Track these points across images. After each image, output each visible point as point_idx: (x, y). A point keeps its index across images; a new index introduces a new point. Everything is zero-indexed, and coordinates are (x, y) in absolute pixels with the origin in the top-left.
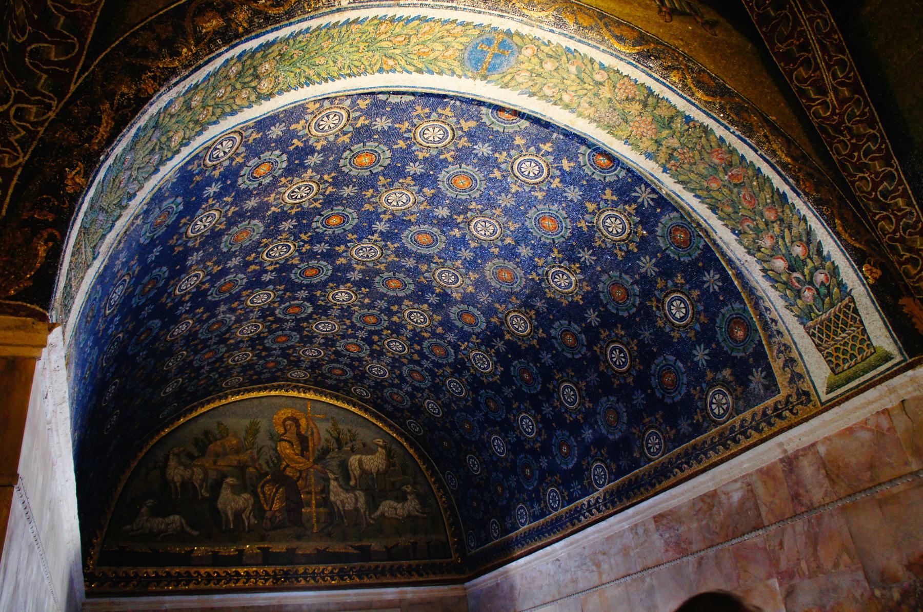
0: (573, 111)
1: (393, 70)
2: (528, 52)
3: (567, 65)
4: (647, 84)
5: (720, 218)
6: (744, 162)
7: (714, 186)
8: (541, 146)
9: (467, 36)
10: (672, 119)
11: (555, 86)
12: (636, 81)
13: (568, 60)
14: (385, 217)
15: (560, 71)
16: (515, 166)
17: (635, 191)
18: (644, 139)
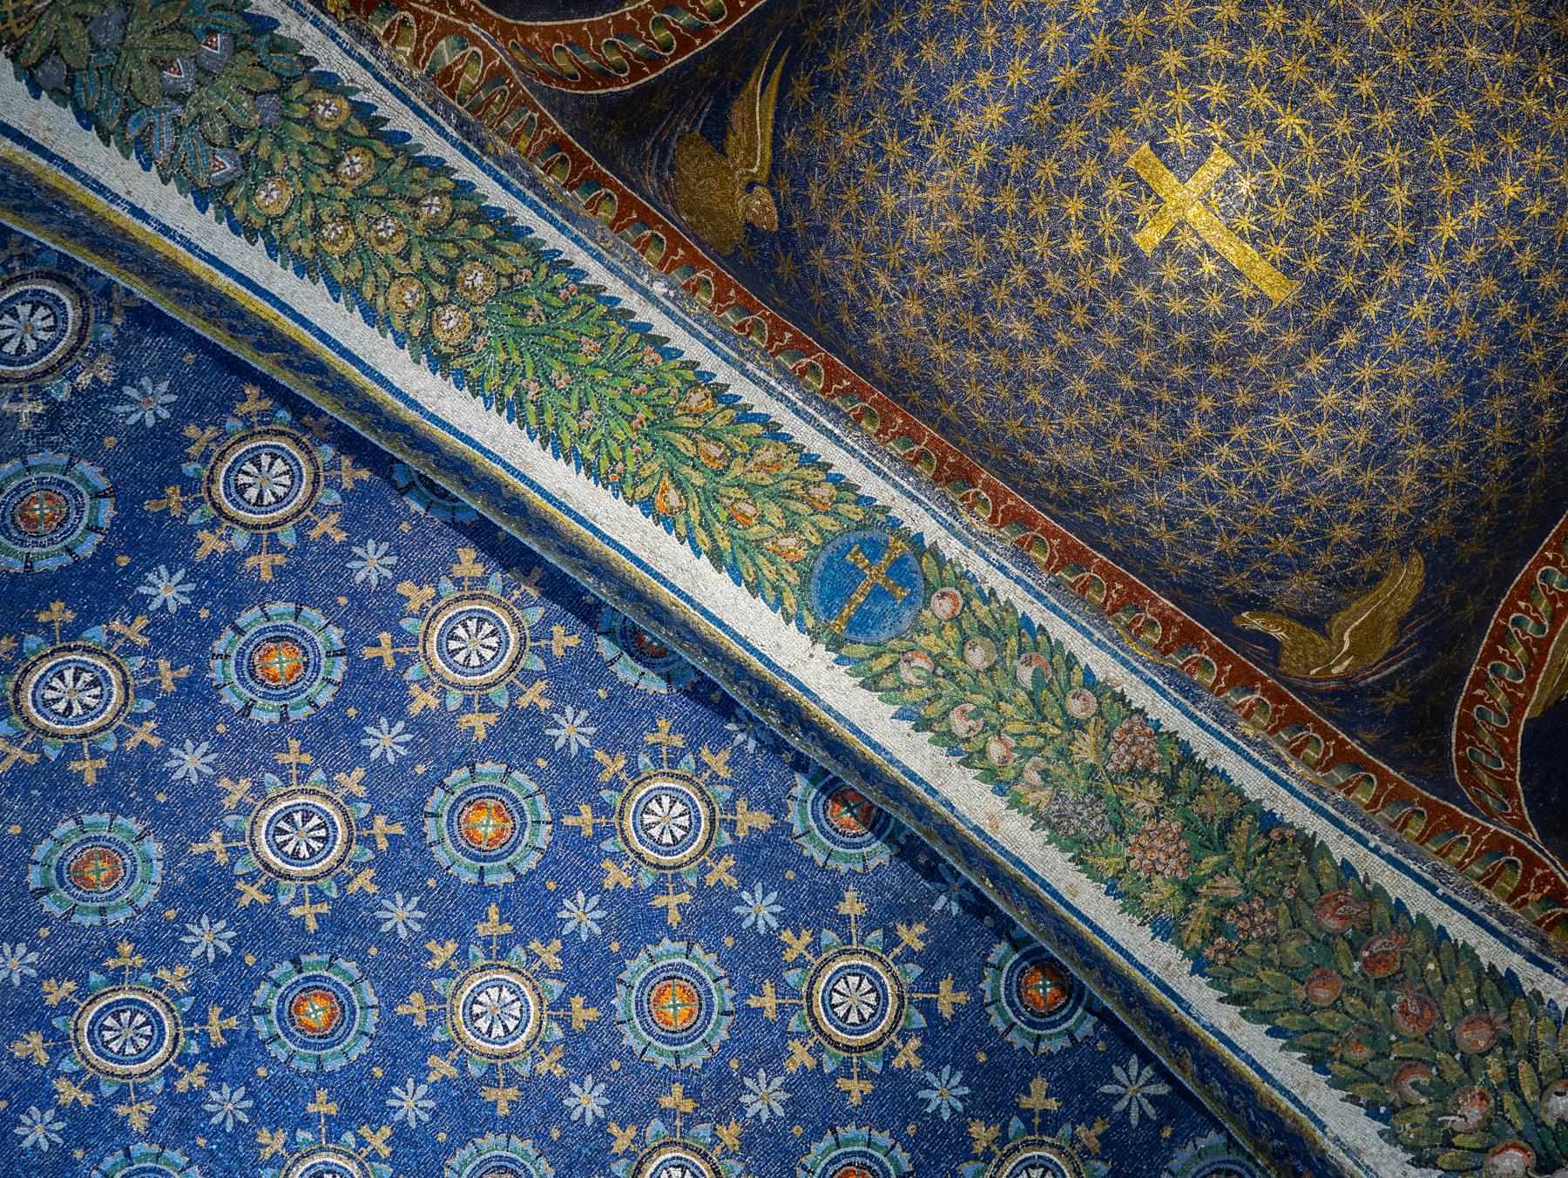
0: (1000, 791)
1: (666, 521)
2: (943, 607)
3: (1016, 663)
4: (1182, 736)
5: (1336, 1084)
6: (1402, 919)
8: (902, 930)
9: (836, 514)
10: (1228, 826)
11: (978, 713)
12: (1158, 725)
13: (1021, 652)
14: (442, 1067)
15: (998, 674)
16: (821, 985)
17: (1112, 1079)
18: (1158, 880)
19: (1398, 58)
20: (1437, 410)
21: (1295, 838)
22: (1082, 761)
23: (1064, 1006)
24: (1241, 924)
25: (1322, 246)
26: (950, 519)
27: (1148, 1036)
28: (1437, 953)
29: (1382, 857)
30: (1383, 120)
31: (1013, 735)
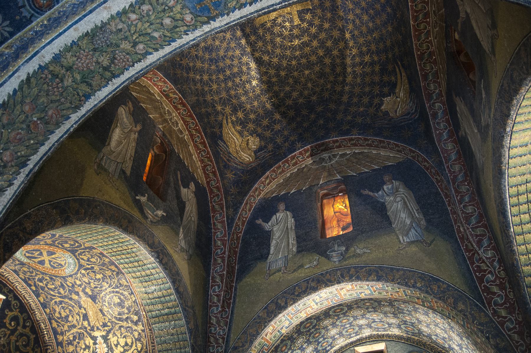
0: (118, 13)
2: (188, 17)
3: (161, 33)
4: (121, 76)
7: (27, 108)
11: (148, 15)
12: (127, 69)
13: (165, 36)
18: (75, 59)
19: (296, 73)
20: (211, 50)
21: (81, 104)
22: (122, 44)
23: (35, 6)
24: (54, 84)
25: (263, 35)
26: (216, 31)
27: (20, 37)
28: (37, 144)
29: (70, 128)
30: (285, 63)
31: (137, 24)
